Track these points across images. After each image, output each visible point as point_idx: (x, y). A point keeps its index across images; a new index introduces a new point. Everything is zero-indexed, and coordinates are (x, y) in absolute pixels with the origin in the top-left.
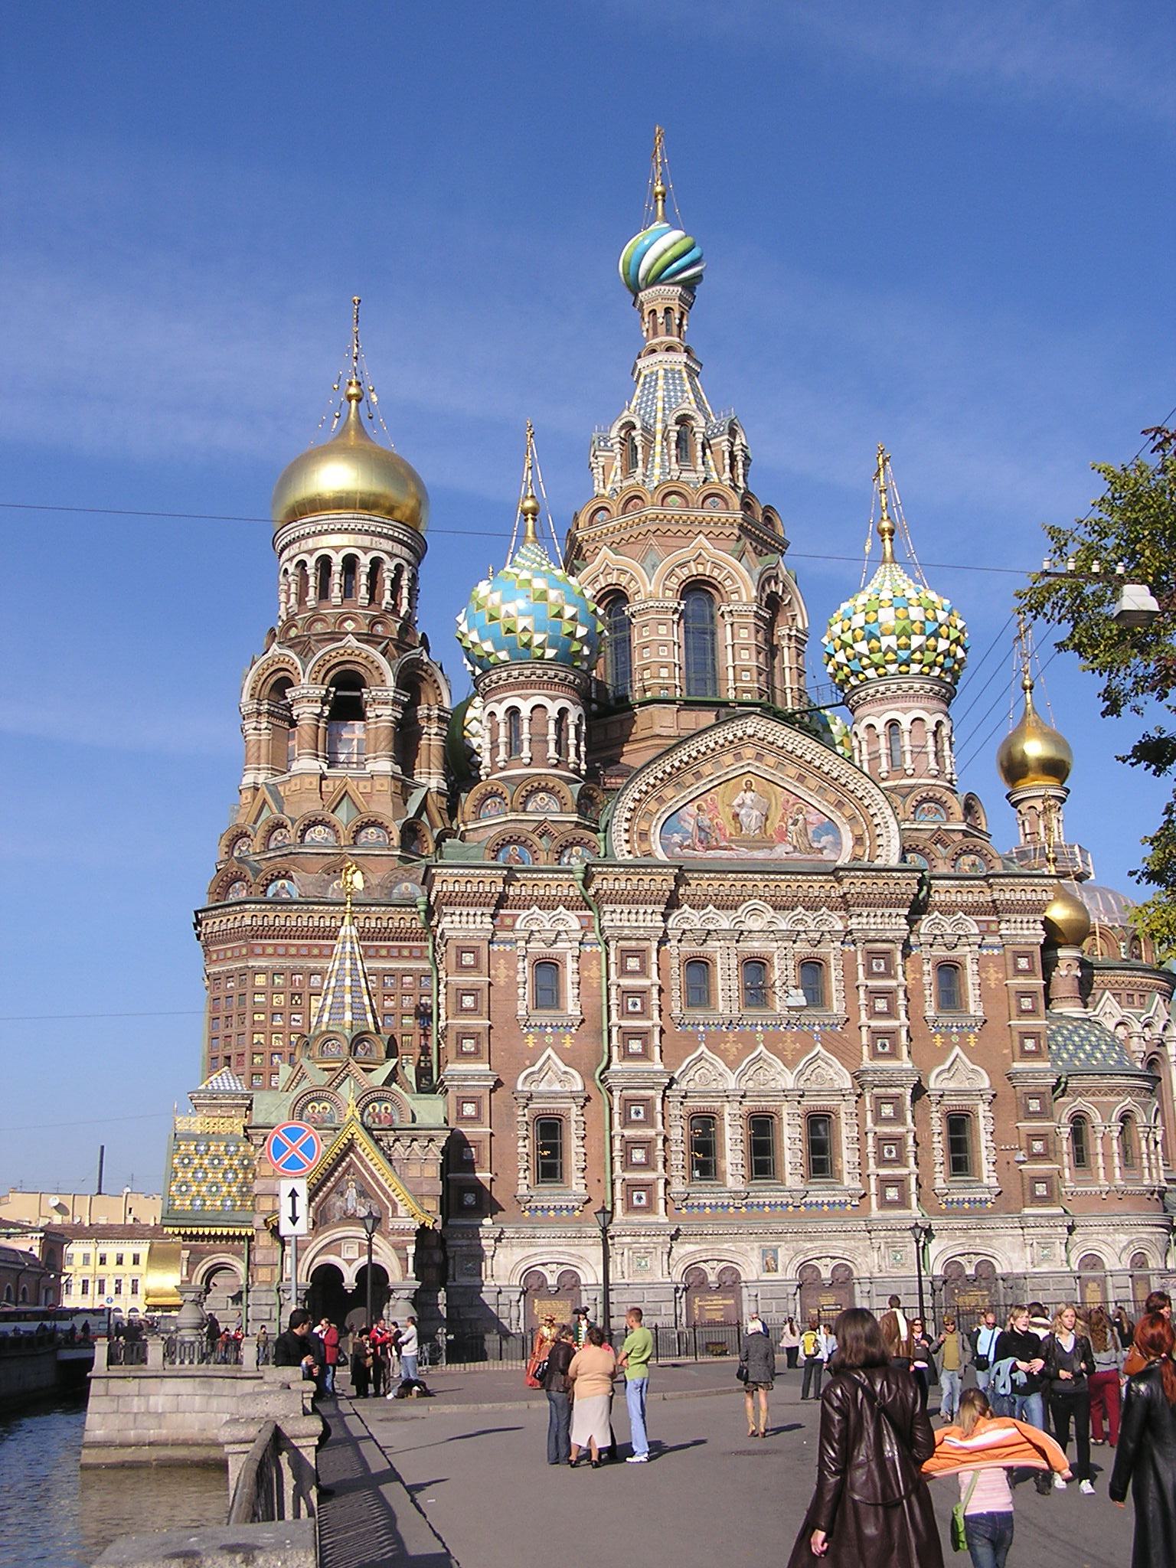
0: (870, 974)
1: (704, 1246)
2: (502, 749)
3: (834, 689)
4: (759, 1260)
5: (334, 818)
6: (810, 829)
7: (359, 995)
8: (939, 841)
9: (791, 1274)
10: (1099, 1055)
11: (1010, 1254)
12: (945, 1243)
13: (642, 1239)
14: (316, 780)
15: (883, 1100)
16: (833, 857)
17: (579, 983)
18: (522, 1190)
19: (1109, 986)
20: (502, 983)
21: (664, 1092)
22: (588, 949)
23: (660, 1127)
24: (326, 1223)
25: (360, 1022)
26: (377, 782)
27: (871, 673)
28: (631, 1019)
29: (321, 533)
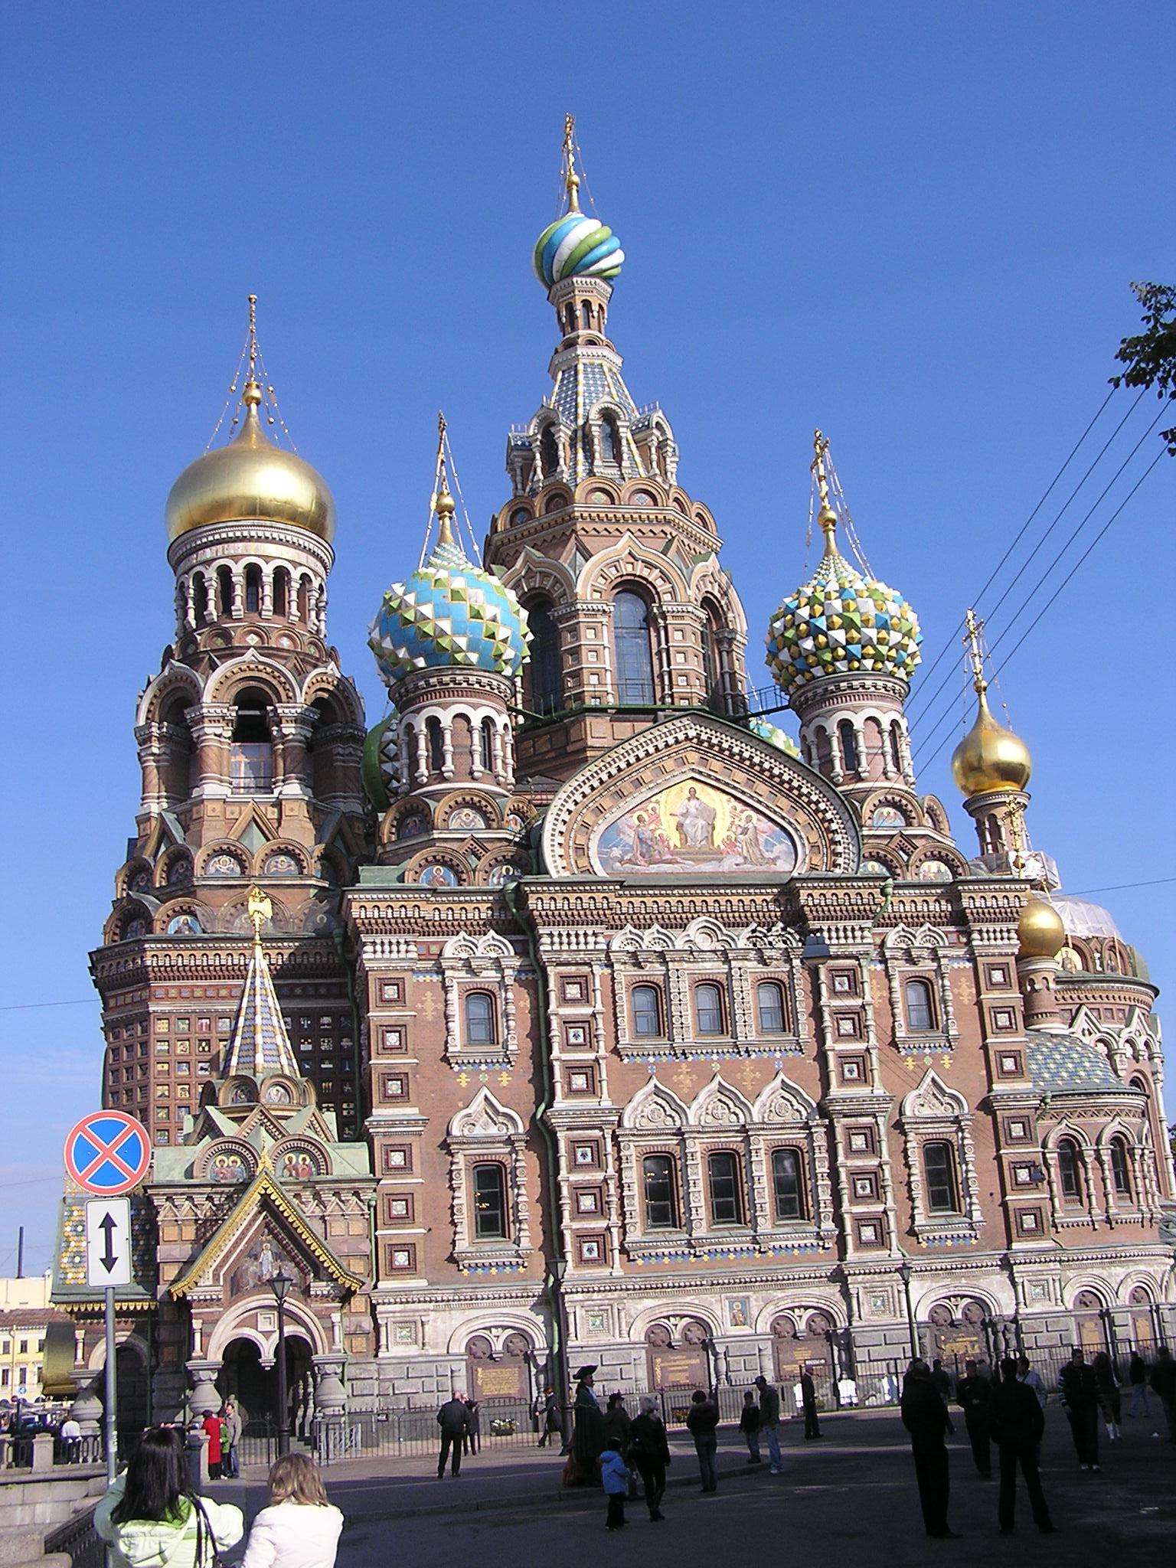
0: (834, 993)
1: (665, 1301)
2: (423, 763)
3: (778, 692)
4: (727, 1315)
6: (762, 838)
9: (764, 1326)
10: (1082, 1074)
11: (999, 1295)
12: (928, 1284)
13: (595, 1296)
15: (854, 1131)
16: (788, 867)
18: (463, 1245)
19: (1085, 1001)
20: (430, 1018)
21: (614, 1132)
22: (523, 977)
23: (611, 1171)
24: (238, 1291)
25: (272, 1065)
26: (287, 807)
27: (818, 671)
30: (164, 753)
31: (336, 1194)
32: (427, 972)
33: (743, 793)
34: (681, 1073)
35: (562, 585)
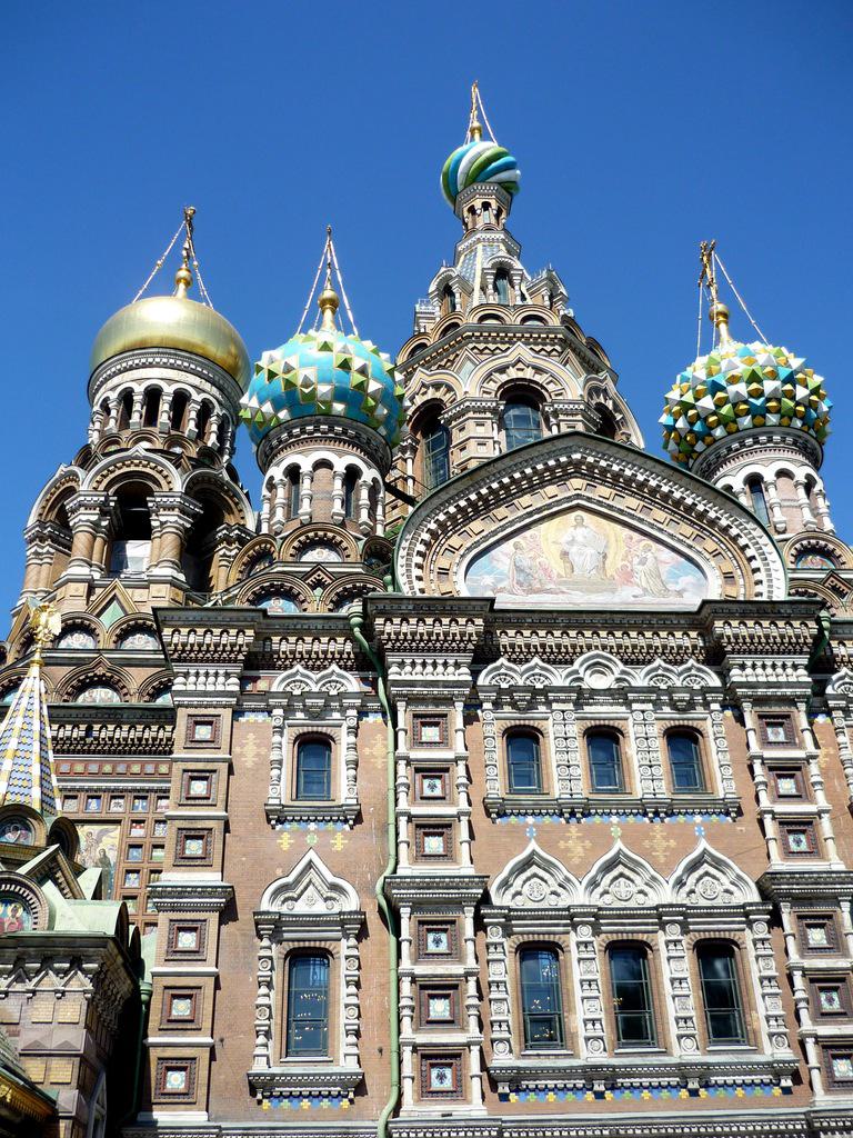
0: (766, 743)
5: (94, 623)
6: (664, 569)
7: (25, 761)
8: (835, 589)
14: (83, 588)
15: (809, 921)
17: (356, 763)
23: (471, 963)
27: (718, 432)
28: (430, 805)
29: (126, 370)
30: (48, 552)
31: (47, 962)
32: (253, 711)
33: (641, 520)
34: (569, 838)
35: (453, 390)
